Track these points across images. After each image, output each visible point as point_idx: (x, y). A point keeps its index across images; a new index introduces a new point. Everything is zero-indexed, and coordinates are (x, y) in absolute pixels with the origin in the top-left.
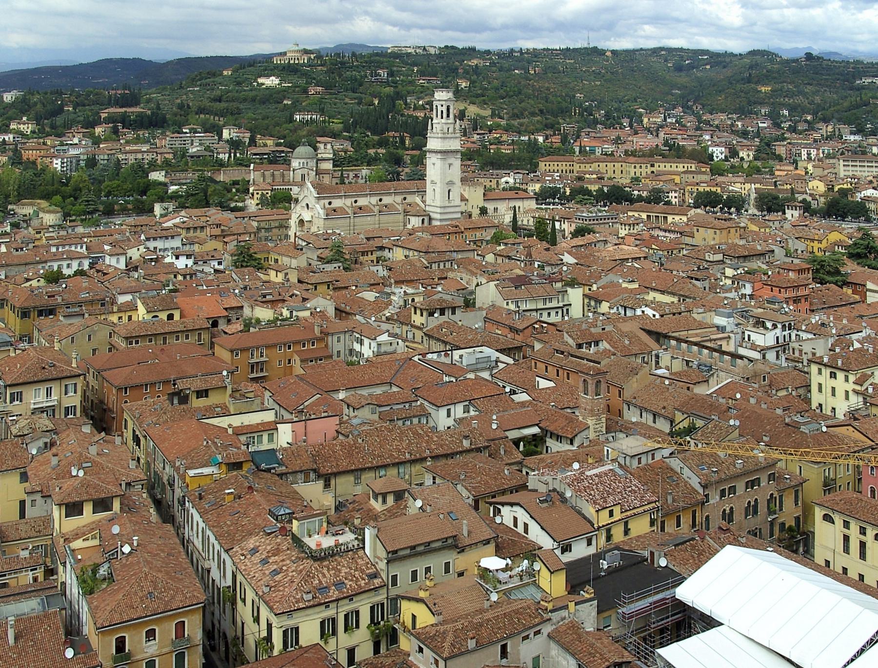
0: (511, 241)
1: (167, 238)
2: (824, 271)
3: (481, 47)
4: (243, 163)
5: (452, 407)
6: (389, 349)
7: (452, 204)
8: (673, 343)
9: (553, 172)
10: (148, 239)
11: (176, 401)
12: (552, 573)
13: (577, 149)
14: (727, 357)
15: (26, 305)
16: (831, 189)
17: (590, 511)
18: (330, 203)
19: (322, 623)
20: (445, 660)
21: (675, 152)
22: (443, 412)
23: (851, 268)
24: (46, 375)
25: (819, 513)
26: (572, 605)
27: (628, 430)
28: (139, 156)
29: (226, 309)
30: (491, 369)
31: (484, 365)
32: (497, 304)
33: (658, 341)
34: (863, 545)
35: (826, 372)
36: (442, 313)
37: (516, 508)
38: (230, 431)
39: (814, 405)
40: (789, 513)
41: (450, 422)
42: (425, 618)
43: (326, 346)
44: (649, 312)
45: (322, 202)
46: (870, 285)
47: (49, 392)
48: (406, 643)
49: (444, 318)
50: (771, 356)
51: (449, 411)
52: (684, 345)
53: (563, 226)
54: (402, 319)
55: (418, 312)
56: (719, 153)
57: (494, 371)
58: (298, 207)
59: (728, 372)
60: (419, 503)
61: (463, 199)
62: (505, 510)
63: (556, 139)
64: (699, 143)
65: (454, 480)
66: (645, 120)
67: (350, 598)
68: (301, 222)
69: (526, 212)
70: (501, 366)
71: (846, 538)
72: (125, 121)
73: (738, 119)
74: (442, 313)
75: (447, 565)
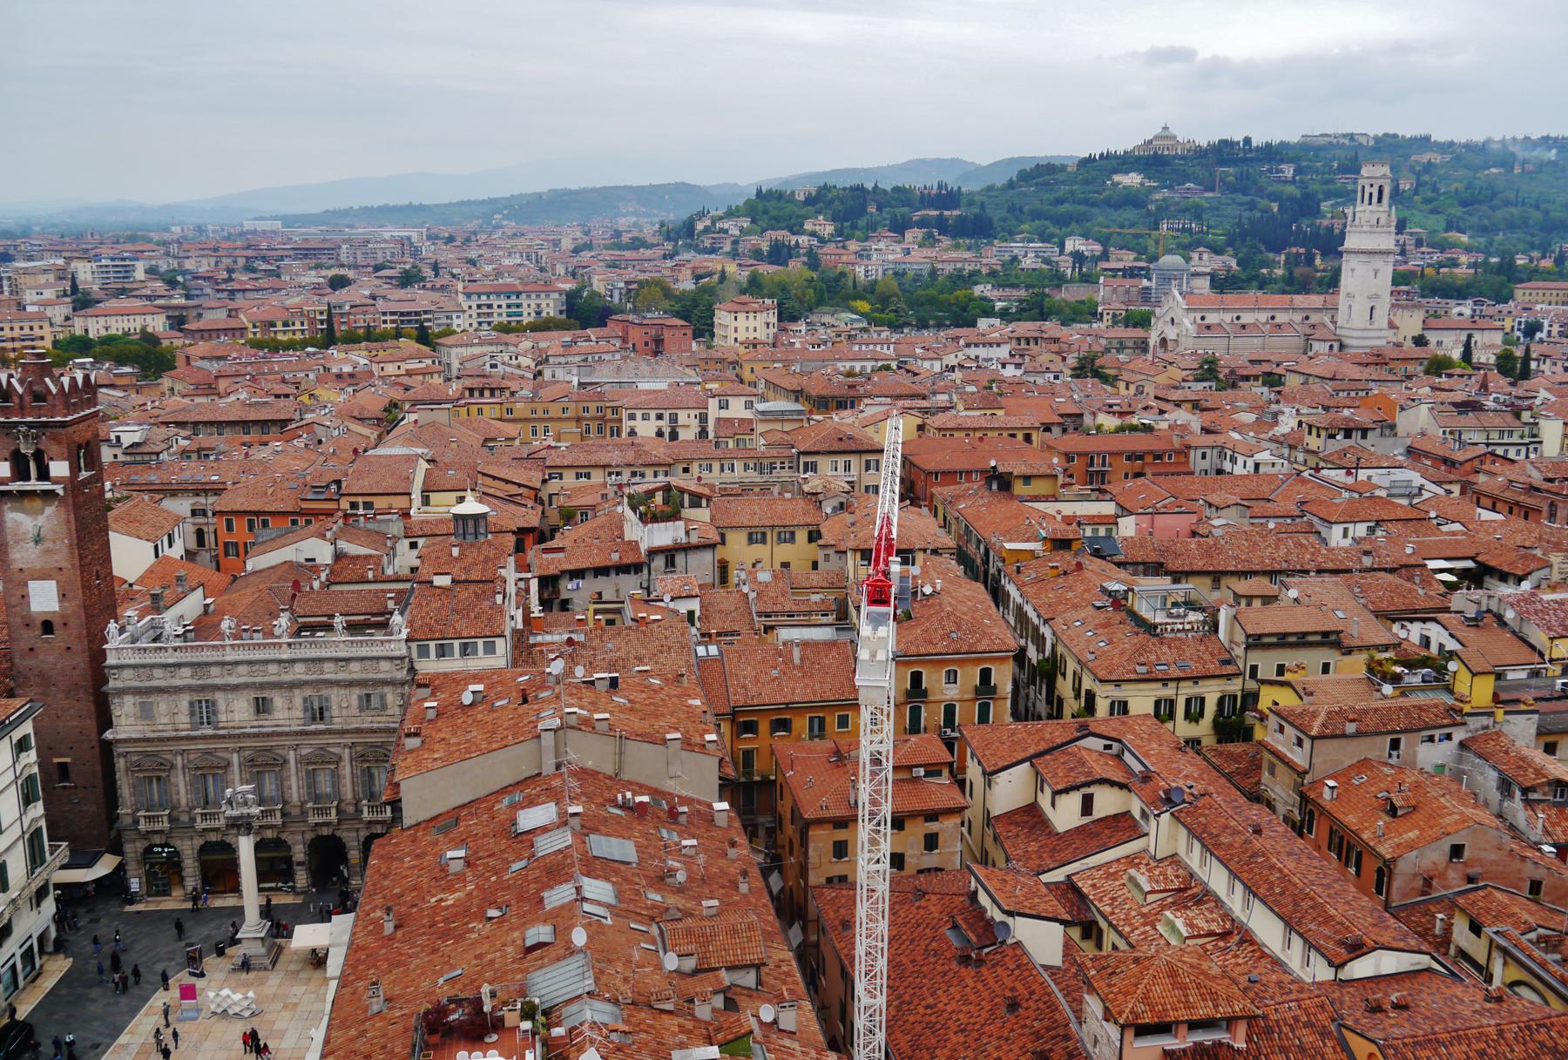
0: (1458, 371)
1: (991, 345)
3: (1439, 136)
4: (1088, 279)
5: (1351, 526)
6: (1270, 470)
7: (1376, 326)
10: (968, 345)
11: (995, 487)
12: (1474, 675)
15: (823, 393)
17: (1539, 637)
18: (1203, 318)
19: (1157, 703)
20: (1313, 738)
22: (1337, 530)
24: (842, 446)
26: (1500, 713)
28: (959, 265)
29: (1062, 415)
30: (1410, 496)
31: (1402, 491)
32: (1429, 432)
36: (1348, 435)
37: (1429, 625)
38: (1059, 518)
41: (1347, 543)
43: (1187, 462)
45: (1192, 315)
47: (847, 467)
49: (1348, 442)
51: (1346, 530)
53: (1542, 367)
54: (1290, 443)
55: (1314, 431)
57: (1415, 501)
58: (1160, 324)
61: (1392, 326)
67: (1195, 680)
68: (1164, 342)
69: (1487, 347)
70: (1426, 495)
72: (943, 226)
74: (1348, 435)
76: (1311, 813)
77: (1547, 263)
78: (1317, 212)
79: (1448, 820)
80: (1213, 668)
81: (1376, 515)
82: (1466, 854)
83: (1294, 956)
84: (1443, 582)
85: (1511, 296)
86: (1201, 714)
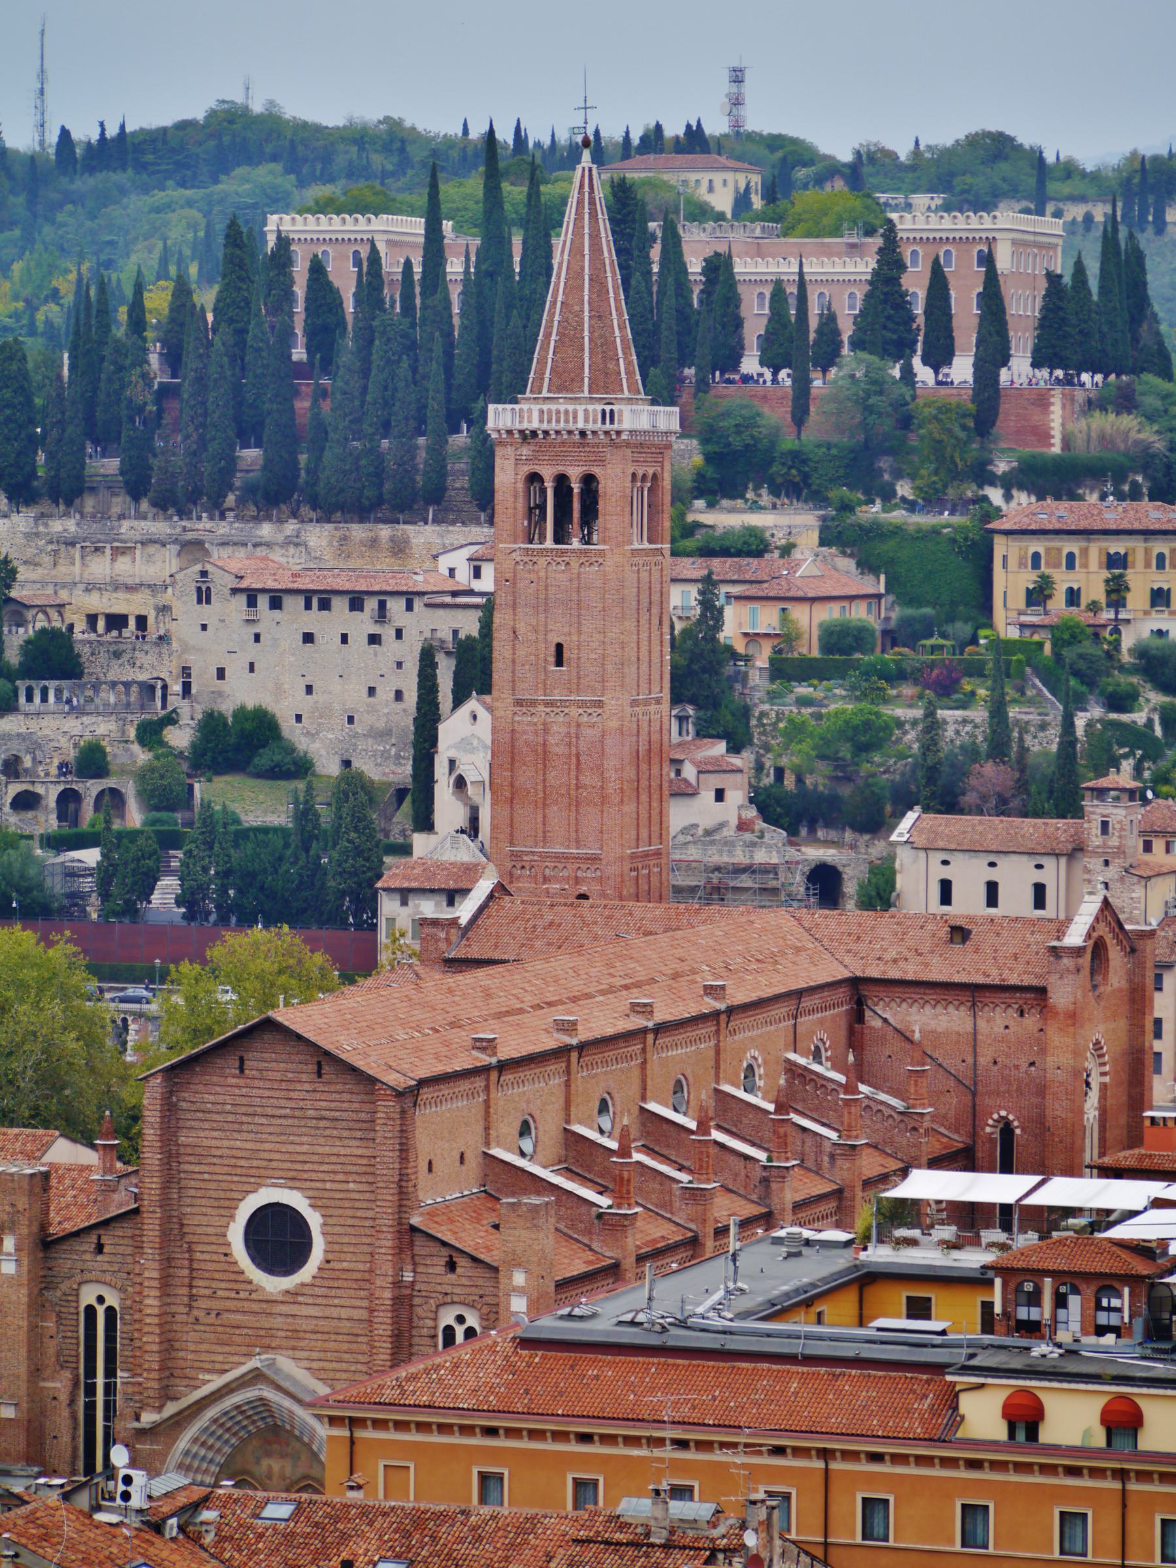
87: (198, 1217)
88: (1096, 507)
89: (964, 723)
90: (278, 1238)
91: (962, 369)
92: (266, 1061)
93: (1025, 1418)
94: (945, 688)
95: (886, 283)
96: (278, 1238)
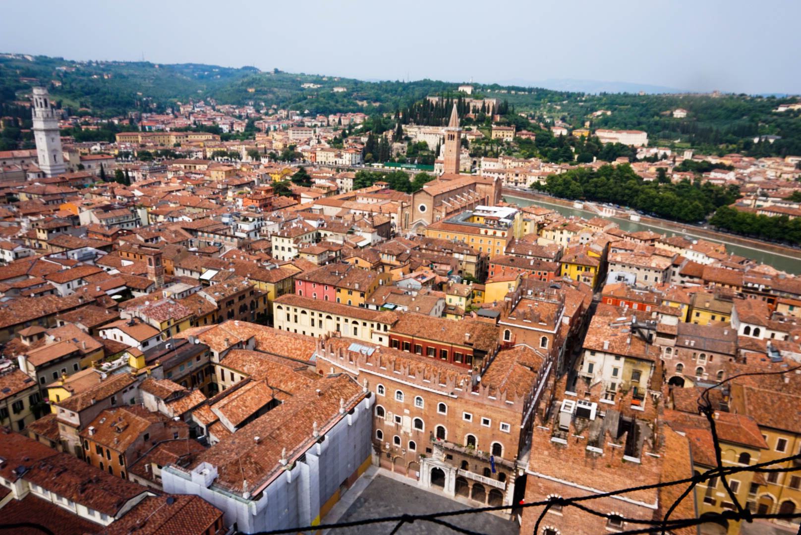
2: (280, 189)
8: (200, 233)
9: (123, 143)
13: (140, 128)
14: (229, 238)
16: (285, 146)
21: (199, 129)
23: (294, 187)
25: (275, 305)
27: (177, 280)
30: (93, 259)
33: (191, 233)
34: (296, 317)
35: (280, 239)
39: (274, 256)
40: (262, 306)
42: (64, 395)
44: (186, 219)
46: (302, 195)
48: (55, 410)
50: (252, 235)
52: (206, 234)
56: (226, 129)
59: (230, 245)
60: (53, 337)
62: (108, 332)
63: (126, 122)
64: (214, 122)
65: (73, 321)
66: (182, 109)
70: (100, 256)
71: (288, 315)
73: (237, 108)
75: (76, 366)
76: (86, 442)
77: (126, 122)
78: (14, 98)
79: (141, 426)
80: (22, 386)
81: (80, 275)
82: (150, 436)
83: (96, 518)
84: (116, 300)
85: (115, 139)
86: (22, 408)
87: (415, 206)
88: (502, 127)
89: (488, 148)
90: (423, 208)
91: (490, 114)
92: (423, 193)
93: (486, 232)
94: (487, 144)
95: (484, 107)
96: (423, 208)
